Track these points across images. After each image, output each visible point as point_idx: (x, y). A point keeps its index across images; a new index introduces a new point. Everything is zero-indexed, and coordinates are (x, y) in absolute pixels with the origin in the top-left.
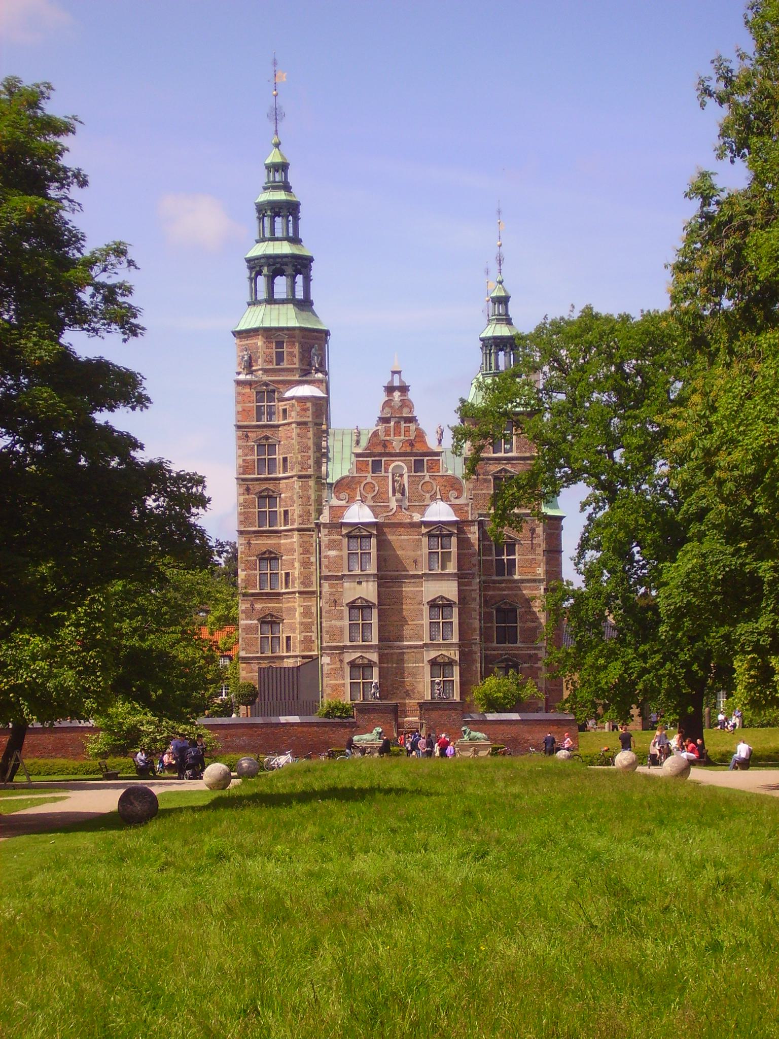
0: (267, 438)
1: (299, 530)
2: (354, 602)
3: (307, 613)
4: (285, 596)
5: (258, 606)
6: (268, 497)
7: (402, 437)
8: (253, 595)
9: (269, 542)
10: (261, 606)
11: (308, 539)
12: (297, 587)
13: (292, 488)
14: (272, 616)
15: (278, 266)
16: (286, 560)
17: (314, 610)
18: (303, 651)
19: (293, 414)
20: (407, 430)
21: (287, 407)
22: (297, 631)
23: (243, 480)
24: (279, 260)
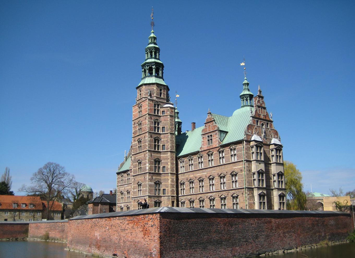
0: (157, 120)
1: (170, 152)
2: (259, 171)
3: (172, 181)
4: (162, 174)
5: (154, 178)
6: (157, 140)
7: (263, 114)
8: (152, 173)
9: (157, 155)
10: (155, 178)
11: (172, 155)
12: (169, 172)
13: (167, 137)
14: (158, 181)
15: (158, 66)
16: (163, 162)
17: (175, 180)
18: (172, 194)
19: (168, 113)
20: (264, 112)
21: (165, 110)
22: (170, 187)
23: (150, 133)
24: (158, 65)
